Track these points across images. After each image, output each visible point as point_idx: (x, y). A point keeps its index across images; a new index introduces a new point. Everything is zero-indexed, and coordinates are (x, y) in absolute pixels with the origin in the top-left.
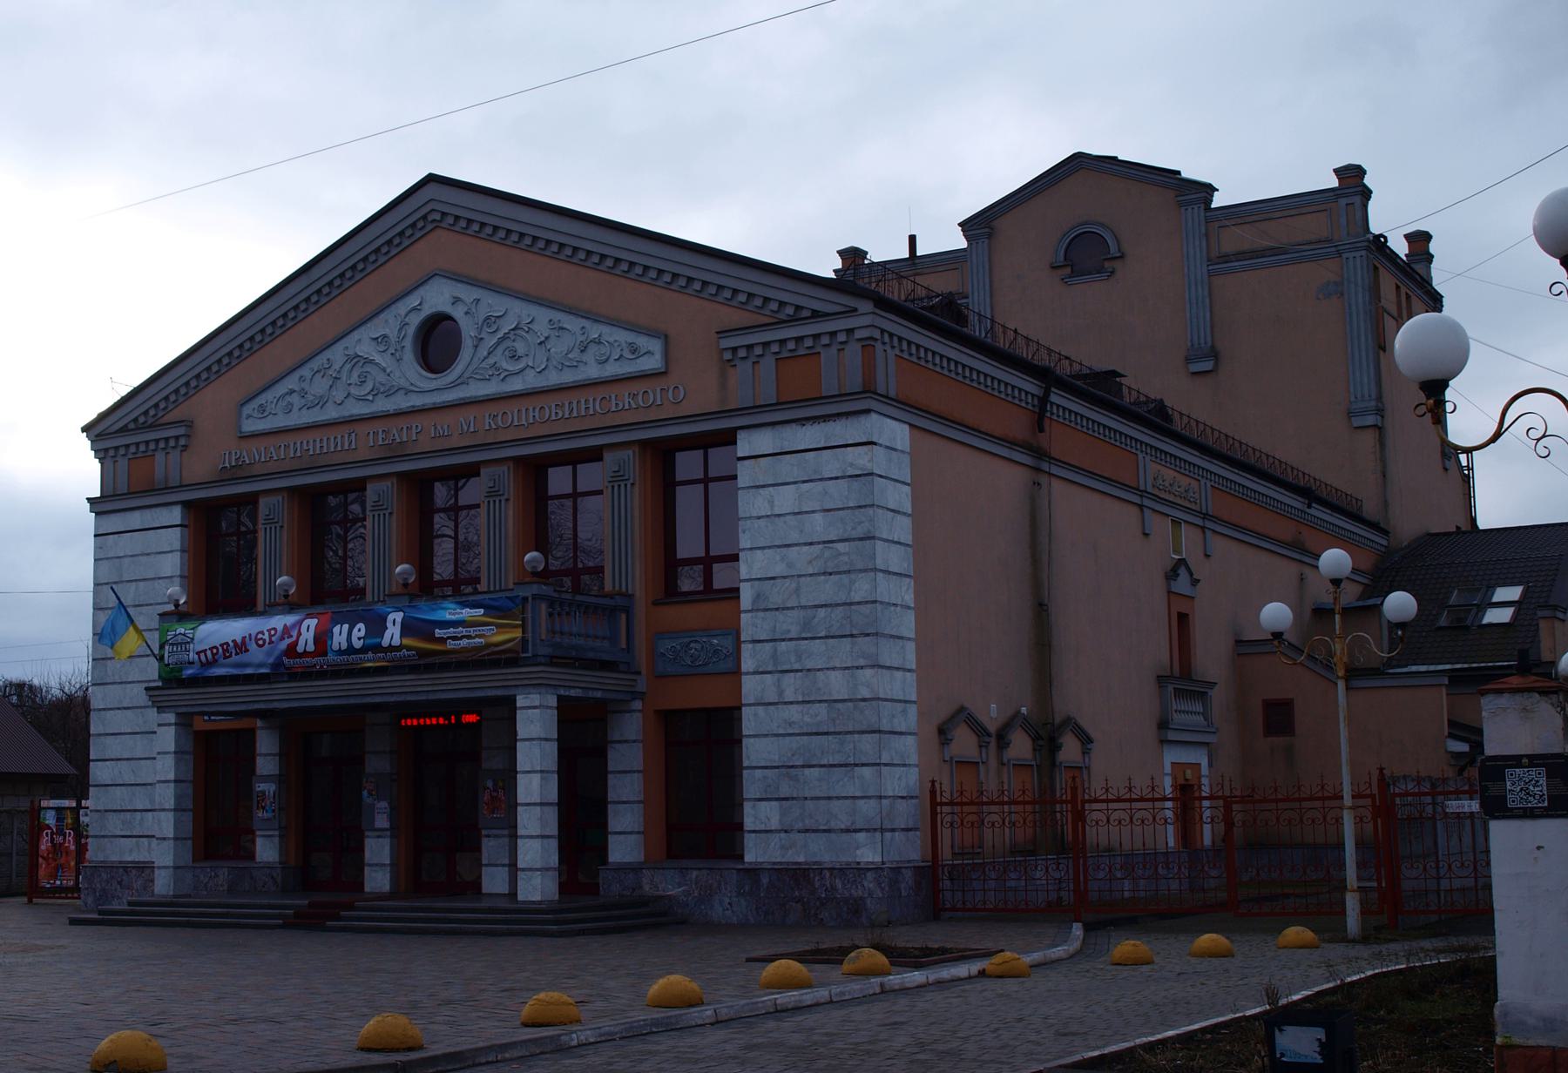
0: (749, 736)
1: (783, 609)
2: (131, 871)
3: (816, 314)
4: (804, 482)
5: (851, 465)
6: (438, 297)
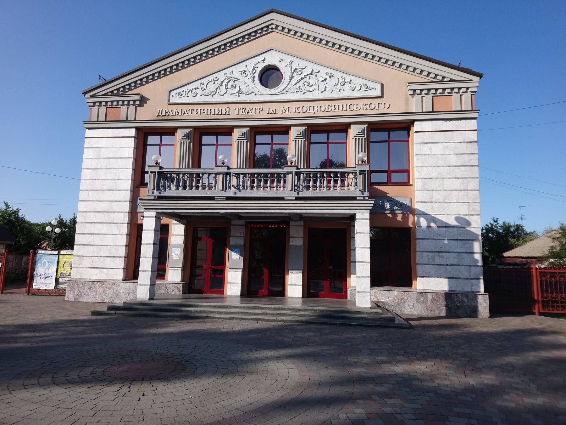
1: (436, 190)
2: (96, 283)
3: (451, 80)
4: (446, 143)
6: (272, 59)
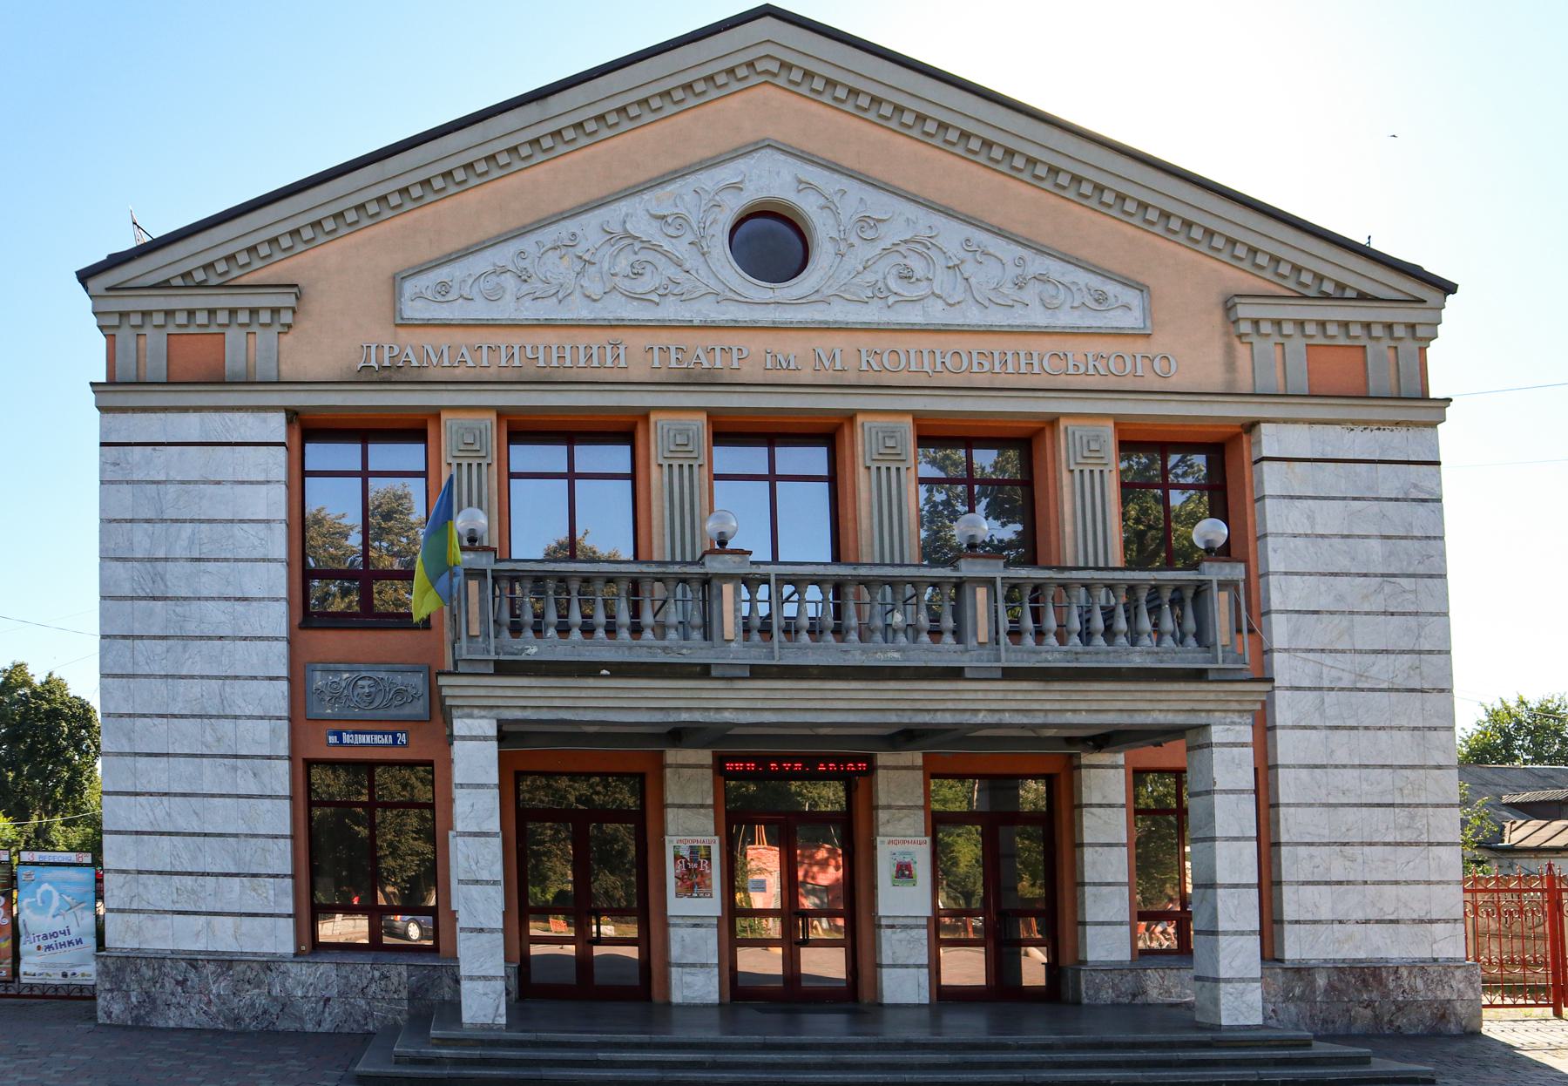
0: (1288, 805)
1: (1331, 651)
2: (205, 966)
3: (1362, 297)
5: (1415, 486)
